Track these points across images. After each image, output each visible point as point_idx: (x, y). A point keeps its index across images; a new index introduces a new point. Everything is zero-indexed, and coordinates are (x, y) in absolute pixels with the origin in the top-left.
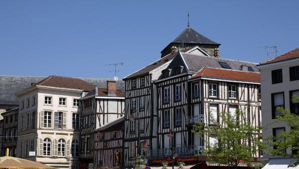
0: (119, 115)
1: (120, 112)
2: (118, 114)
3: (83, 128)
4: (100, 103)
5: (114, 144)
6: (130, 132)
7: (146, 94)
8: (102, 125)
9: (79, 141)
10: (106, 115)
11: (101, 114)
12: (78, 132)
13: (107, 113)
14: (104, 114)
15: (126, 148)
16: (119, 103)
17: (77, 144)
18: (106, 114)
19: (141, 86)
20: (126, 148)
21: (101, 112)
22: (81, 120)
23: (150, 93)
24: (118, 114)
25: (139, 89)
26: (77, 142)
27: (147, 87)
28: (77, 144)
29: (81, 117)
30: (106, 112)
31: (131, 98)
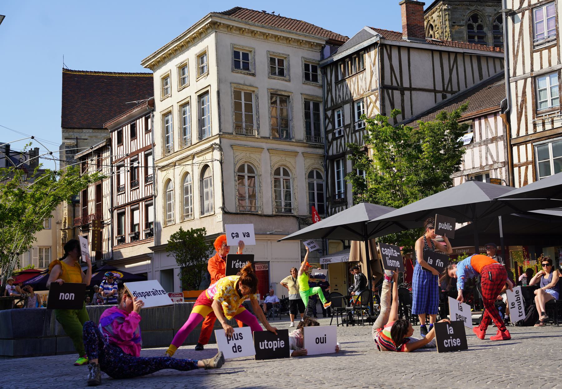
0: (439, 96)
1: (439, 87)
2: (435, 91)
3: (334, 138)
9: (323, 175)
10: (407, 93)
11: (396, 89)
12: (320, 151)
13: (411, 89)
14: (402, 90)
17: (320, 181)
18: (407, 89)
21: (395, 84)
22: (326, 117)
24: (435, 91)
26: (319, 176)
28: (320, 181)
29: (325, 110)
30: (406, 84)
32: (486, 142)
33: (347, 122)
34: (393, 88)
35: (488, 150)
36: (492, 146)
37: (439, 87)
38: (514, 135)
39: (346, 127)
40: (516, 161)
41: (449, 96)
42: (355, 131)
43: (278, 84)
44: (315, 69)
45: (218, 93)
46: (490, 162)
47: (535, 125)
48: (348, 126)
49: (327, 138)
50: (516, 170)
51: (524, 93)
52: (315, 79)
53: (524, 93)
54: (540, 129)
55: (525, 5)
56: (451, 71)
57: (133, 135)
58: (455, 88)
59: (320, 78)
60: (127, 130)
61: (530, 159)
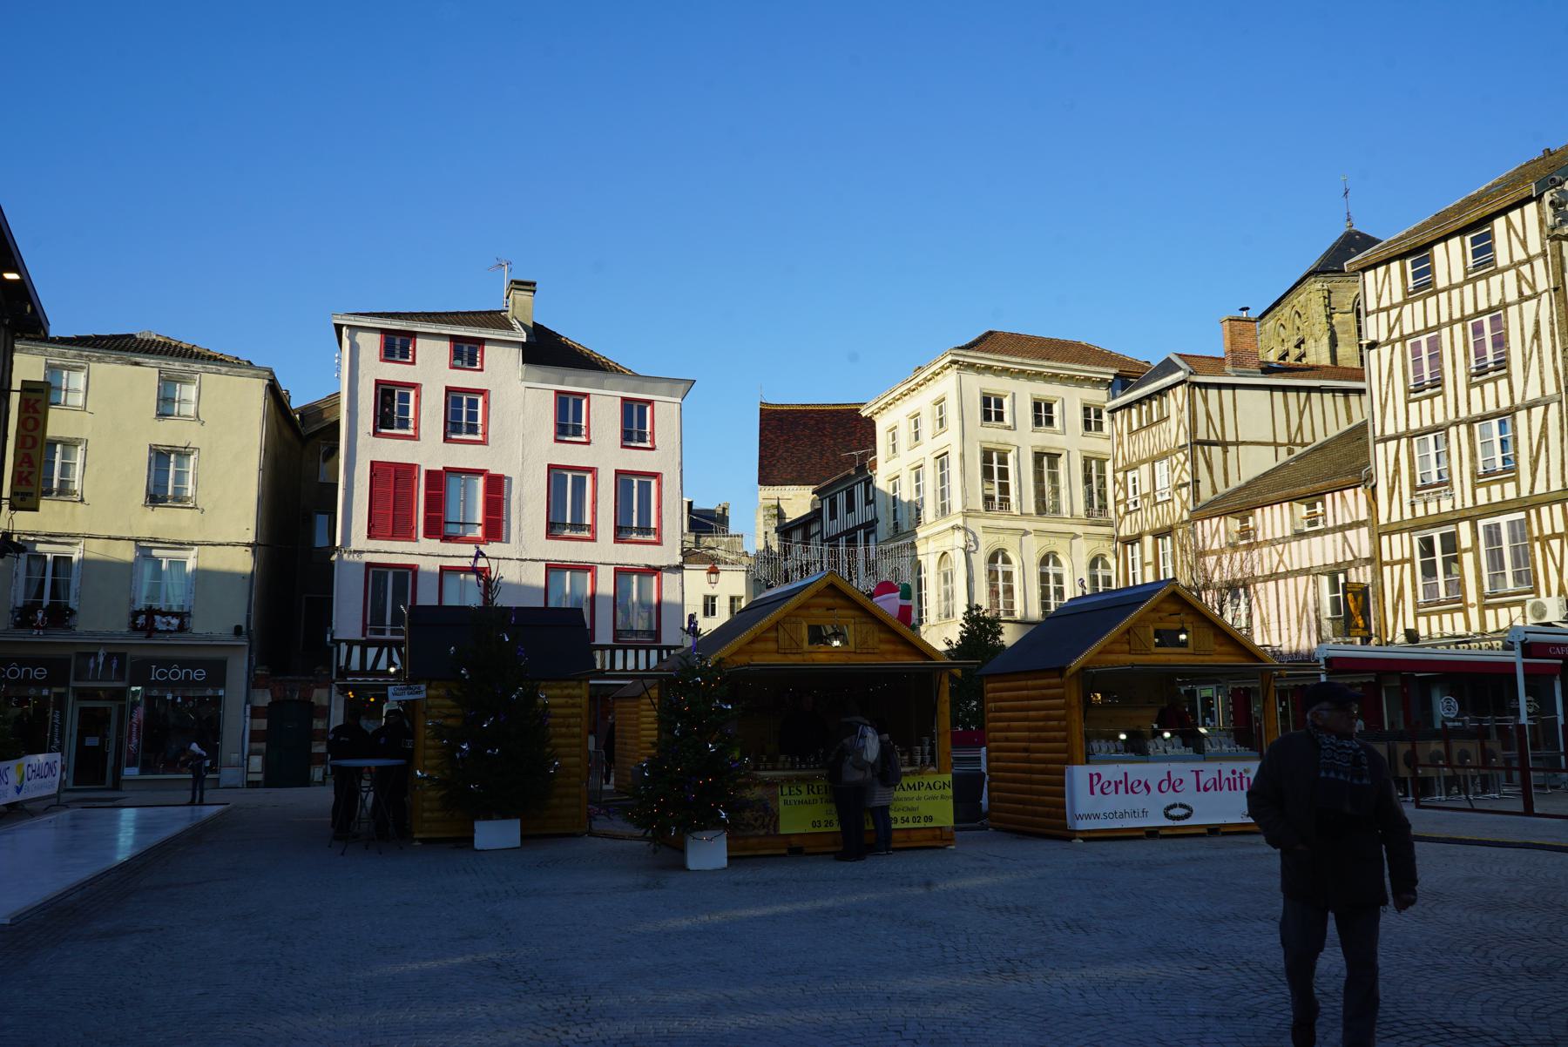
0: (1283, 451)
1: (1282, 438)
2: (1276, 444)
3: (1128, 512)
4: (1205, 400)
5: (1324, 550)
6: (1414, 488)
7: (1512, 296)
8: (1221, 489)
10: (1232, 449)
13: (1237, 443)
14: (1224, 445)
15: (1392, 563)
16: (1278, 395)
17: (1106, 573)
18: (1232, 444)
19: (1466, 273)
20: (1392, 563)
21: (1213, 438)
23: (1542, 284)
24: (1276, 444)
25: (1460, 286)
27: (1515, 265)
31: (1403, 338)
32: (1343, 528)
33: (1146, 489)
34: (1211, 444)
35: (1345, 539)
36: (1350, 534)
37: (1282, 438)
38: (1383, 520)
39: (1143, 496)
40: (1386, 557)
41: (1298, 451)
42: (1156, 504)
43: (1045, 439)
44: (1099, 415)
45: (962, 456)
46: (1349, 557)
47: (1413, 505)
48: (1147, 495)
49: (1116, 511)
50: (1387, 569)
51: (1397, 459)
52: (1099, 427)
53: (1397, 459)
54: (1420, 512)
55: (1396, 335)
56: (1301, 414)
57: (850, 507)
58: (1308, 438)
59: (1106, 426)
60: (841, 499)
61: (1407, 555)
